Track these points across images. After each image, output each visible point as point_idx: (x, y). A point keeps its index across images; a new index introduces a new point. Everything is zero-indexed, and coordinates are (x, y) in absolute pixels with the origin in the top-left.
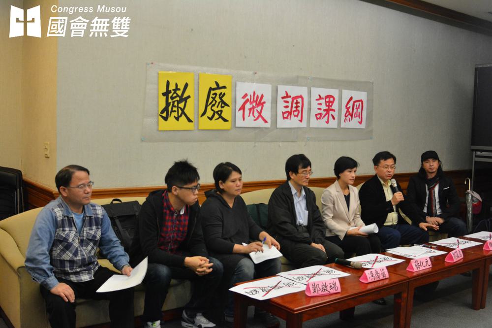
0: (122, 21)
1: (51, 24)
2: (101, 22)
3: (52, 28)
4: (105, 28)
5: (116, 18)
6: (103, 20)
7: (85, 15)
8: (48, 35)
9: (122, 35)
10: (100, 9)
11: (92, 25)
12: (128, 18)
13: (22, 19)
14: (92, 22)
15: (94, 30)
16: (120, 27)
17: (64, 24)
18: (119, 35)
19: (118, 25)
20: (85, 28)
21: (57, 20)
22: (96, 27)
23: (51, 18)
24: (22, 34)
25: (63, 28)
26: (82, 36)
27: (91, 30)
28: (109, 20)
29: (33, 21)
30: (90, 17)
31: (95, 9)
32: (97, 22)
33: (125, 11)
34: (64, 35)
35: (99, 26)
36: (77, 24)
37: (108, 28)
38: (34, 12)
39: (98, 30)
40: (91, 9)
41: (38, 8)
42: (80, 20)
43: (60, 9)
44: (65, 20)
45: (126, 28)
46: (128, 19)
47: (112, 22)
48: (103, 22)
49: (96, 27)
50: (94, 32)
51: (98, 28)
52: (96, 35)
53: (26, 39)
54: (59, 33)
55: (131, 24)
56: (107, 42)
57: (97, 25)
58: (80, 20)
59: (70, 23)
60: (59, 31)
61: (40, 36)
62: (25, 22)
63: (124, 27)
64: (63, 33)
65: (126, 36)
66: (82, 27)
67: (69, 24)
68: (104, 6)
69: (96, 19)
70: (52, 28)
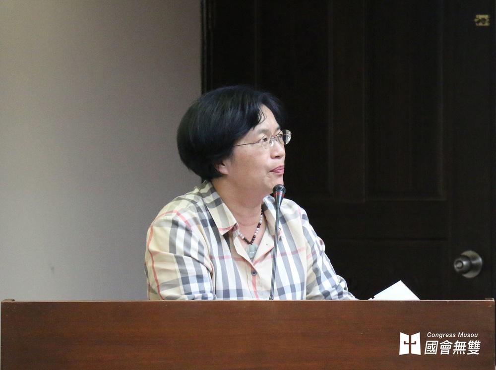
0: (475, 343)
3: (428, 348)
5: (470, 341)
6: (462, 343)
7: (450, 339)
9: (475, 353)
10: (460, 335)
11: (454, 346)
13: (407, 341)
15: (456, 350)
18: (473, 353)
19: (472, 346)
20: (450, 348)
21: (431, 343)
23: (427, 341)
24: (408, 353)
25: (435, 349)
26: (448, 353)
27: (454, 350)
29: (415, 343)
30: (453, 340)
31: (457, 335)
32: (458, 344)
34: (436, 353)
35: (460, 347)
36: (444, 345)
37: (465, 348)
38: (416, 337)
39: (459, 350)
43: (433, 335)
45: (477, 348)
50: (456, 351)
52: (458, 353)
53: (410, 356)
54: (432, 352)
55: (481, 346)
56: (465, 359)
59: (440, 345)
60: (433, 350)
61: (420, 354)
62: (410, 344)
65: (478, 354)
66: (448, 348)
67: (439, 346)
68: (463, 333)
69: (457, 342)
70: (428, 348)
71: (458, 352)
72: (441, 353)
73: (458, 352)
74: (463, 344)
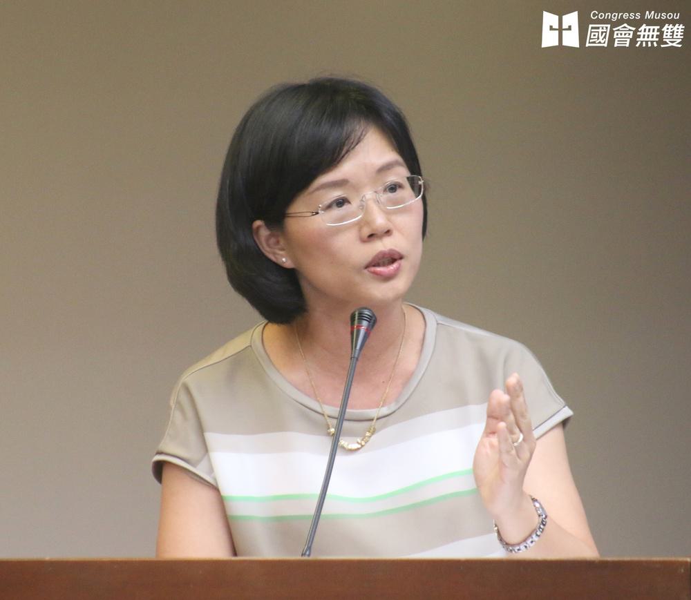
1: (591, 32)
2: (649, 29)
3: (592, 37)
4: (655, 36)
5: (667, 25)
6: (652, 28)
7: (630, 22)
8: (587, 45)
9: (674, 44)
11: (638, 33)
12: (681, 25)
13: (556, 26)
14: (640, 30)
15: (641, 39)
16: (673, 35)
17: (606, 32)
18: (671, 44)
19: (669, 34)
20: (631, 36)
21: (598, 28)
22: (644, 36)
23: (591, 26)
24: (556, 44)
25: (605, 37)
26: (627, 45)
27: (638, 39)
28: (658, 27)
29: (570, 28)
31: (643, 15)
32: (645, 31)
33: (678, 18)
34: (606, 45)
35: (648, 34)
37: (657, 36)
38: (572, 19)
39: (646, 39)
40: (638, 16)
41: (576, 13)
42: (625, 27)
43: (601, 16)
44: (607, 28)
45: (679, 37)
46: (681, 26)
47: (663, 30)
48: (651, 30)
49: (644, 36)
50: (642, 42)
51: (646, 36)
52: (644, 45)
53: (561, 48)
54: (600, 43)
55: (685, 33)
56: (658, 53)
57: (644, 33)
58: (625, 27)
60: (600, 40)
61: (578, 47)
62: (560, 30)
63: (677, 35)
64: (604, 43)
65: (680, 46)
66: (627, 36)
67: (612, 33)
68: (653, 12)
69: (644, 27)
70: (592, 37)
71: (644, 43)
72: (616, 45)
73: (644, 43)
74: (653, 31)
